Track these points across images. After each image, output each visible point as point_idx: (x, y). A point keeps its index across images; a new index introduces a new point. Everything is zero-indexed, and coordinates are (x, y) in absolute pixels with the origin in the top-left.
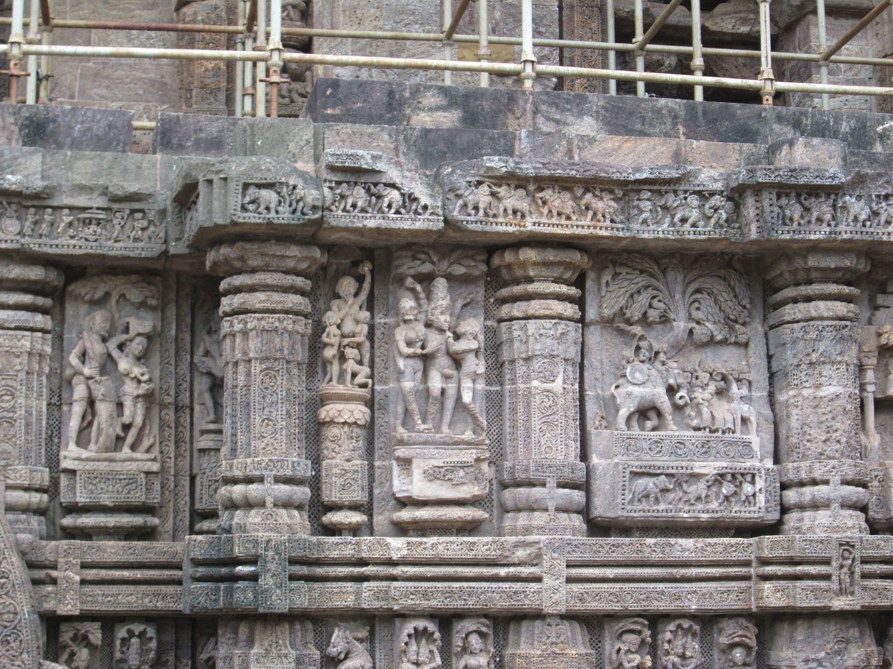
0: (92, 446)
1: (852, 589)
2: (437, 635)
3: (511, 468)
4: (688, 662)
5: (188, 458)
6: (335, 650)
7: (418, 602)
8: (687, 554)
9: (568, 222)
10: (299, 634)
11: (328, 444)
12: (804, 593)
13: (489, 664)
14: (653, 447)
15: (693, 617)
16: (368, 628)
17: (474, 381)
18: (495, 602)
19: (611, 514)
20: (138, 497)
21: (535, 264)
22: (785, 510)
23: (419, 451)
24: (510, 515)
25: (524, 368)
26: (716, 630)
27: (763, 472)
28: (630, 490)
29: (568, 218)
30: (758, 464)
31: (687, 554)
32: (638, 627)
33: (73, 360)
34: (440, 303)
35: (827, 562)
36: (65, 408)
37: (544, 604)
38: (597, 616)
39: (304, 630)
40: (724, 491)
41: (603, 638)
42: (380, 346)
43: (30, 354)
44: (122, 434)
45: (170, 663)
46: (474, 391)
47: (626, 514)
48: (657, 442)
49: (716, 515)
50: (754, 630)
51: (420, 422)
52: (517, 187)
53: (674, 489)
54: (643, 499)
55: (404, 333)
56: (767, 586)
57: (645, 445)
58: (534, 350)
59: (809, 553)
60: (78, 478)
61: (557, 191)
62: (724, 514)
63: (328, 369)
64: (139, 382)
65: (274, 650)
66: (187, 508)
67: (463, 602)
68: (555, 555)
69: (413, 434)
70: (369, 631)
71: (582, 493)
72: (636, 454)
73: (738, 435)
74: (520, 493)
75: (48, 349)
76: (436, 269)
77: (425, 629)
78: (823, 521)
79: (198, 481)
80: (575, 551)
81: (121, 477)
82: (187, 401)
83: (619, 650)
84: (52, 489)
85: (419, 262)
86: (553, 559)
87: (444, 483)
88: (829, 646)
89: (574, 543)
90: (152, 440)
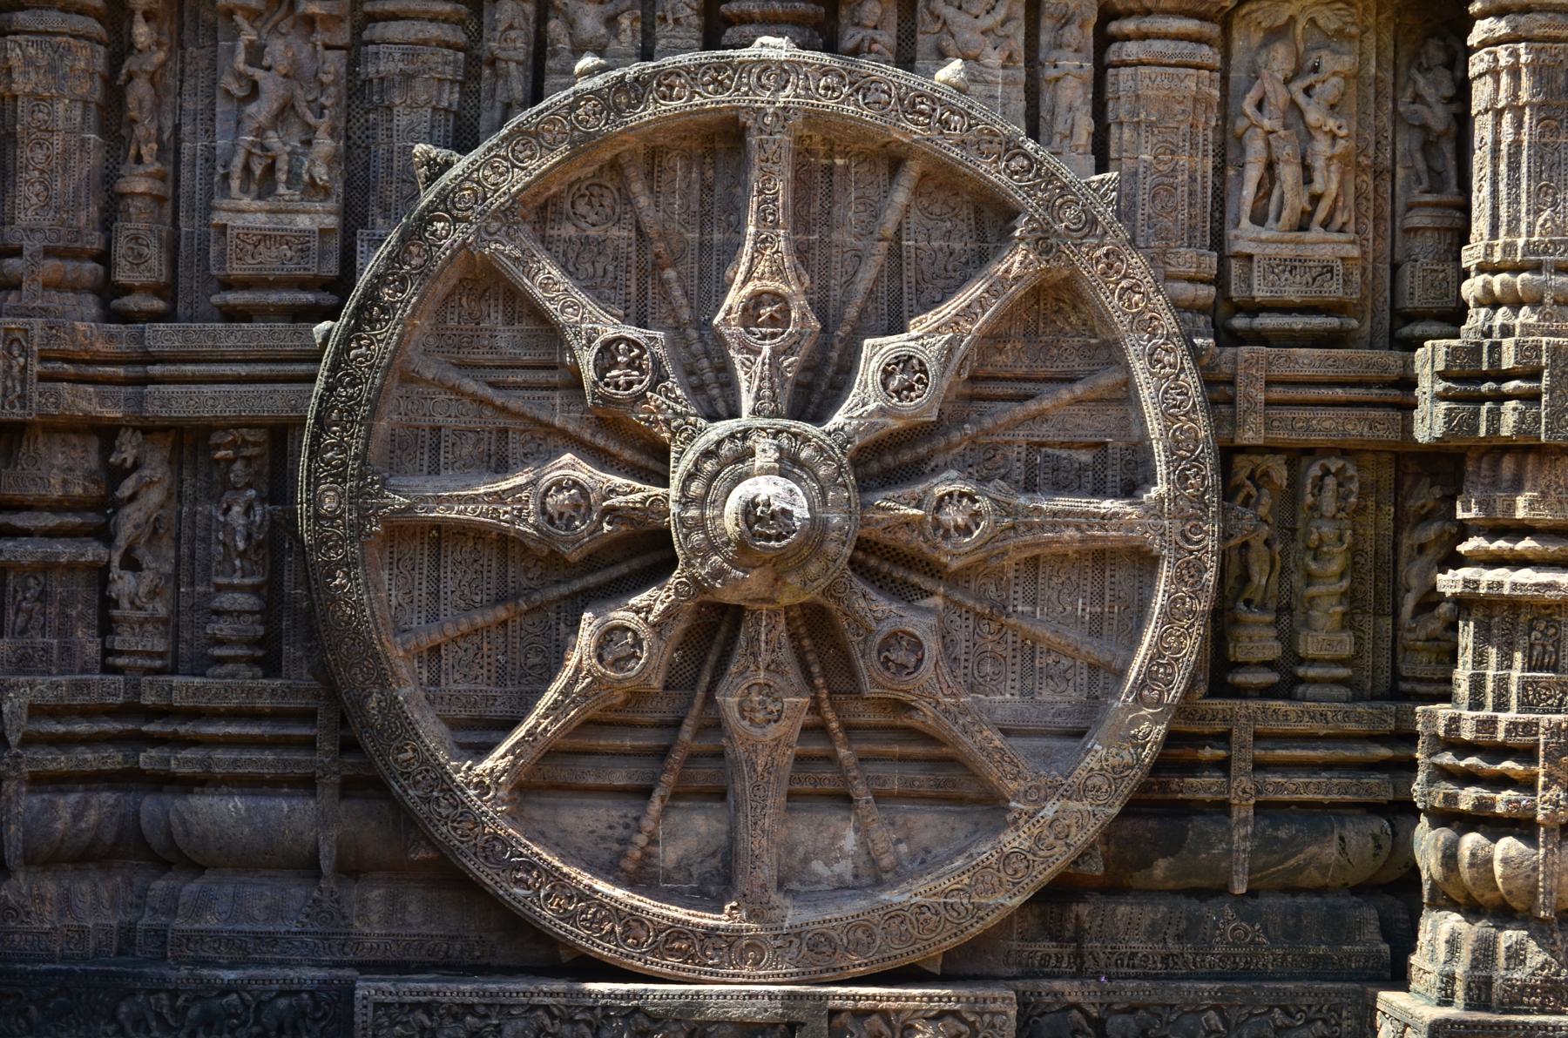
0: (1271, 221)
5: (1389, 240)
20: (1333, 290)
33: (1248, 106)
36: (1231, 172)
43: (1196, 100)
44: (1309, 208)
45: (1369, 511)
60: (1255, 265)
64: (1334, 137)
66: (1387, 308)
75: (1216, 93)
79: (1407, 269)
81: (1311, 264)
82: (1389, 163)
84: (1220, 280)
90: (1345, 218)
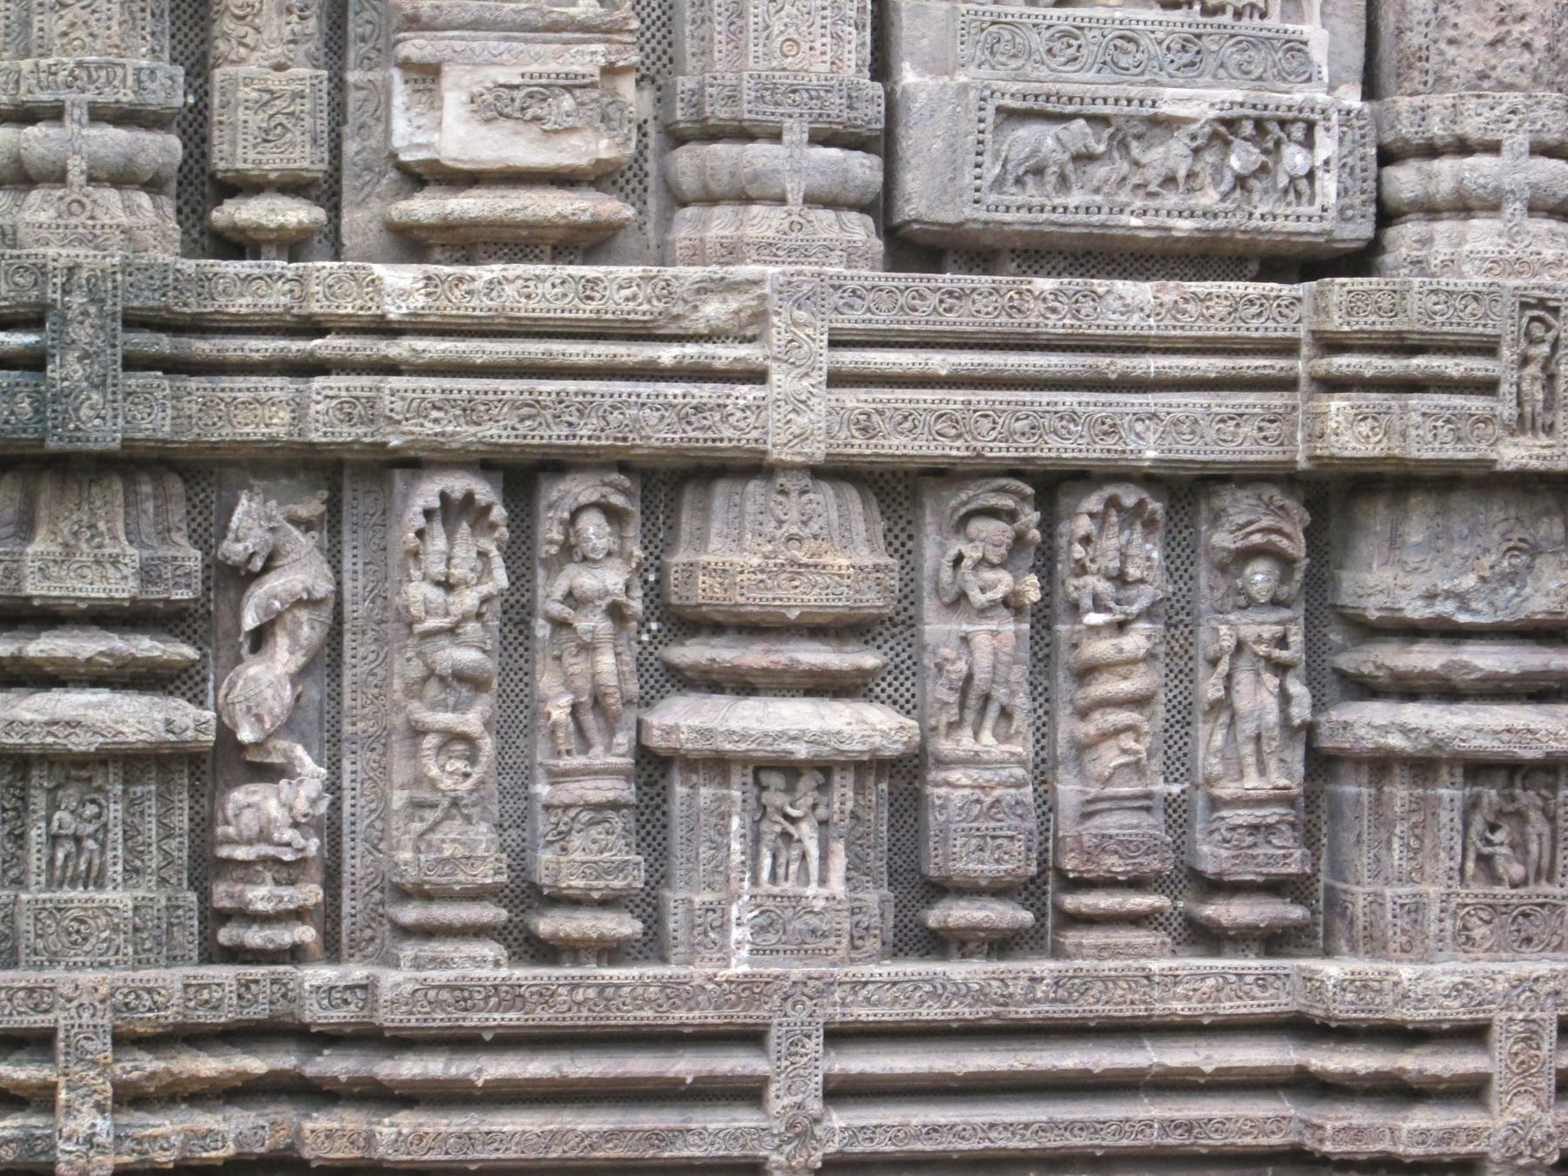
1: (1549, 419)
2: (499, 513)
3: (693, 93)
4: (1132, 592)
6: (239, 547)
7: (450, 429)
8: (1135, 319)
10: (150, 506)
12: (1429, 423)
13: (628, 588)
14: (1057, 46)
15: (1149, 479)
16: (325, 494)
18: (648, 431)
19: (948, 216)
22: (1387, 216)
23: (458, 45)
24: (689, 212)
26: (1204, 514)
27: (1335, 117)
28: (996, 156)
30: (1321, 97)
31: (1135, 319)
32: (1008, 502)
35: (1488, 348)
37: (770, 440)
38: (906, 473)
39: (162, 498)
40: (1235, 162)
41: (920, 529)
47: (983, 215)
48: (1066, 34)
49: (1213, 224)
50: (1300, 516)
53: (1108, 154)
54: (1029, 179)
56: (1337, 405)
57: (1038, 42)
59: (1446, 324)
62: (1234, 222)
65: (84, 546)
67: (565, 431)
68: (802, 315)
70: (328, 502)
71: (874, 161)
72: (1014, 64)
73: (1273, 21)
74: (716, 155)
77: (469, 497)
78: (1481, 246)
80: (851, 307)
83: (958, 560)
86: (796, 324)
87: (521, 127)
88: (1487, 561)
89: (851, 285)
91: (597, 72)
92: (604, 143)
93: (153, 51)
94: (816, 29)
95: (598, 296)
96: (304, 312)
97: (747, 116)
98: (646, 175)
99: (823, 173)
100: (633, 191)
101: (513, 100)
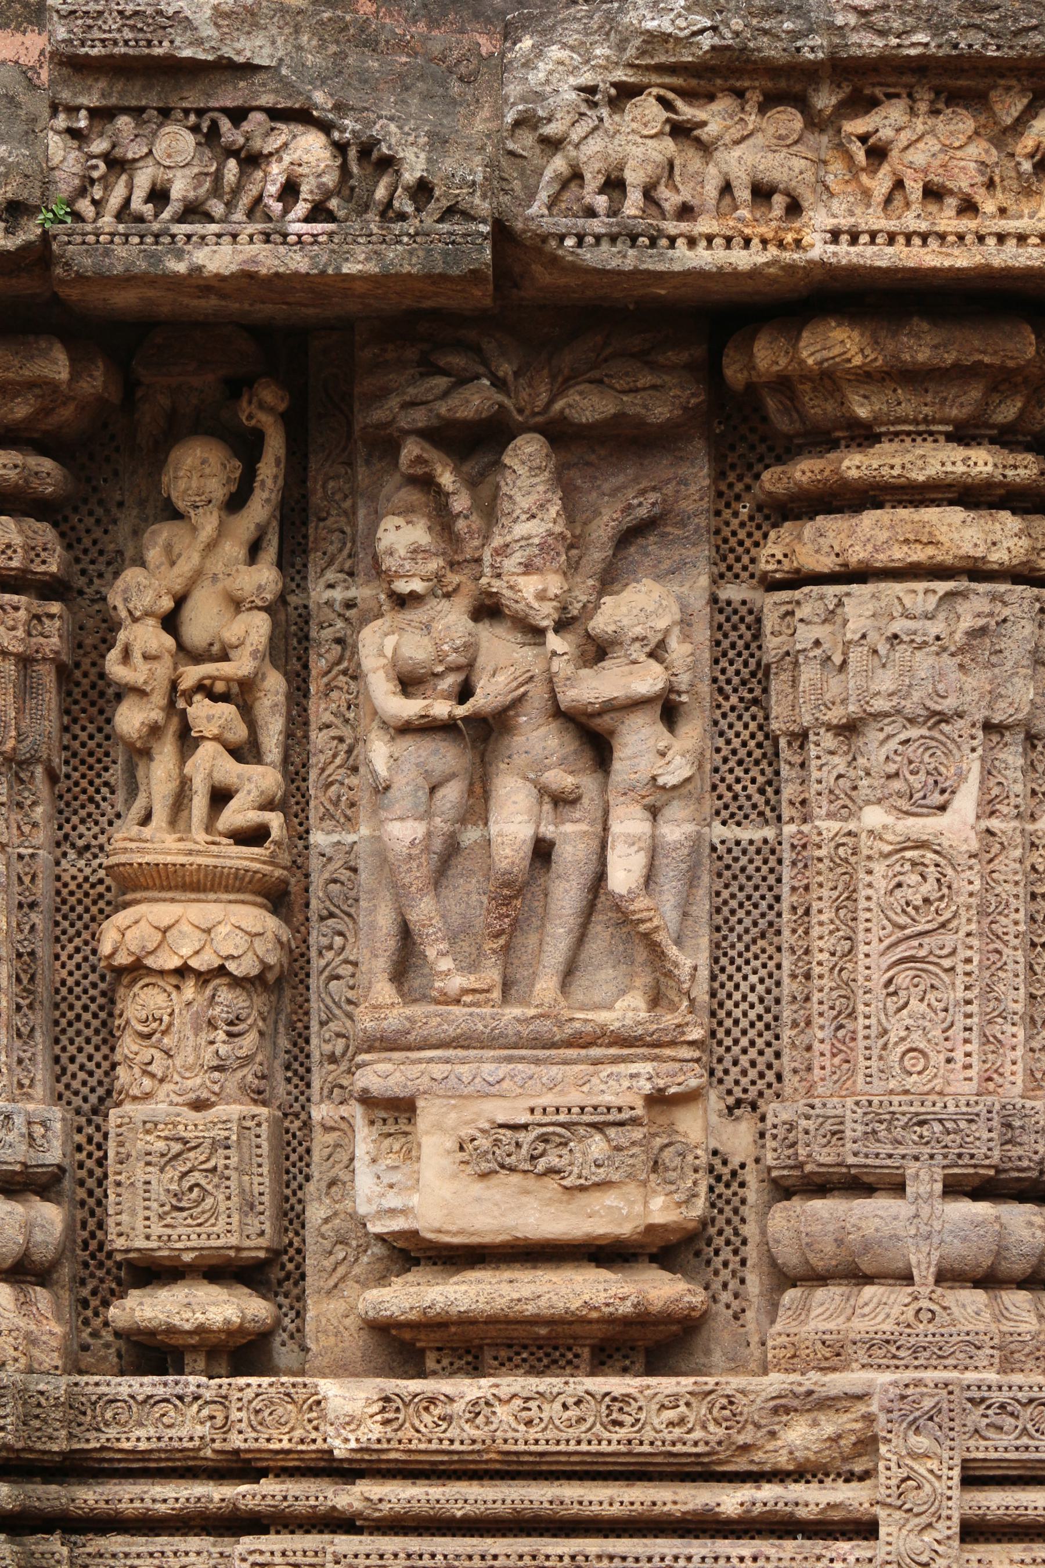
9: (967, 224)
11: (128, 1045)
17: (654, 812)
21: (866, 377)
25: (840, 763)
29: (968, 207)
34: (521, 529)
42: (330, 688)
46: (654, 851)
51: (445, 964)
52: (769, 102)
55: (390, 642)
58: (866, 695)
61: (923, 107)
63: (140, 773)
68: (921, 1442)
69: (418, 1010)
76: (506, 401)
80: (1000, 1428)
85: (442, 382)
86: (913, 1455)
87: (531, 1182)
89: (997, 1397)
91: (639, 1103)
92: (658, 1202)
93: (21, 1086)
94: (957, 1033)
95: (628, 1420)
96: (227, 1447)
97: (851, 1160)
98: (744, 1242)
99: (964, 1239)
100: (726, 1264)
101: (518, 1145)
